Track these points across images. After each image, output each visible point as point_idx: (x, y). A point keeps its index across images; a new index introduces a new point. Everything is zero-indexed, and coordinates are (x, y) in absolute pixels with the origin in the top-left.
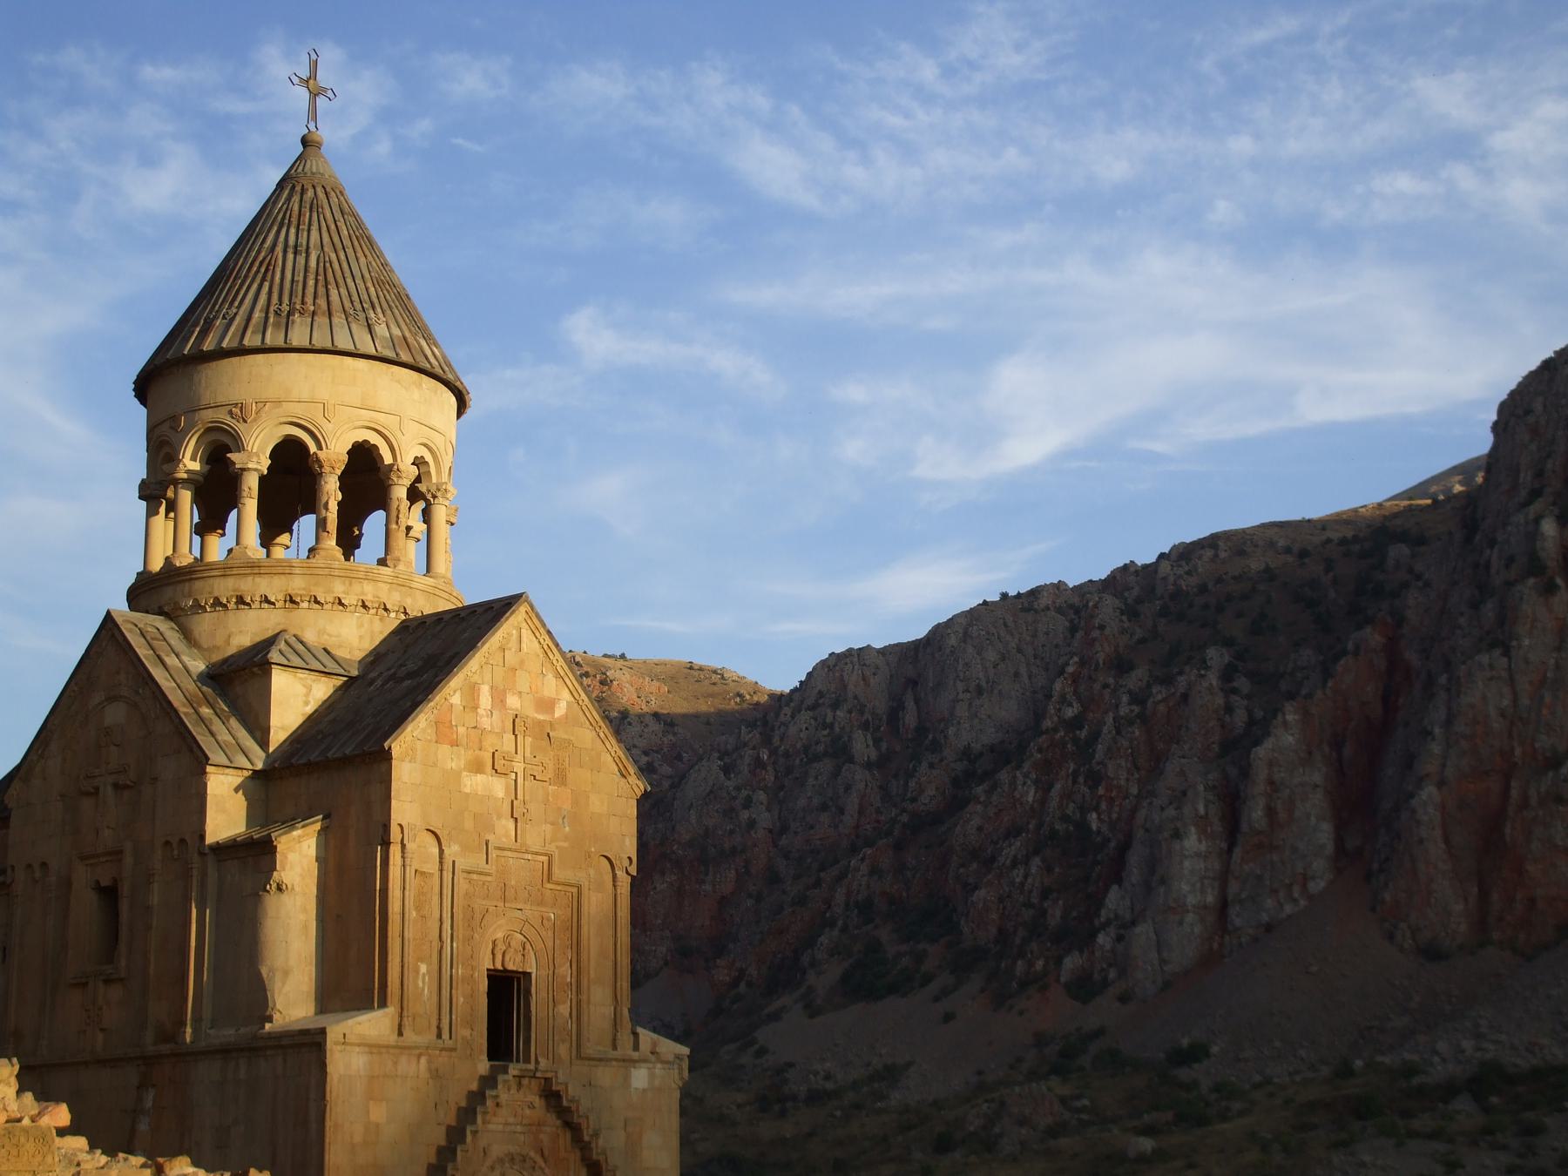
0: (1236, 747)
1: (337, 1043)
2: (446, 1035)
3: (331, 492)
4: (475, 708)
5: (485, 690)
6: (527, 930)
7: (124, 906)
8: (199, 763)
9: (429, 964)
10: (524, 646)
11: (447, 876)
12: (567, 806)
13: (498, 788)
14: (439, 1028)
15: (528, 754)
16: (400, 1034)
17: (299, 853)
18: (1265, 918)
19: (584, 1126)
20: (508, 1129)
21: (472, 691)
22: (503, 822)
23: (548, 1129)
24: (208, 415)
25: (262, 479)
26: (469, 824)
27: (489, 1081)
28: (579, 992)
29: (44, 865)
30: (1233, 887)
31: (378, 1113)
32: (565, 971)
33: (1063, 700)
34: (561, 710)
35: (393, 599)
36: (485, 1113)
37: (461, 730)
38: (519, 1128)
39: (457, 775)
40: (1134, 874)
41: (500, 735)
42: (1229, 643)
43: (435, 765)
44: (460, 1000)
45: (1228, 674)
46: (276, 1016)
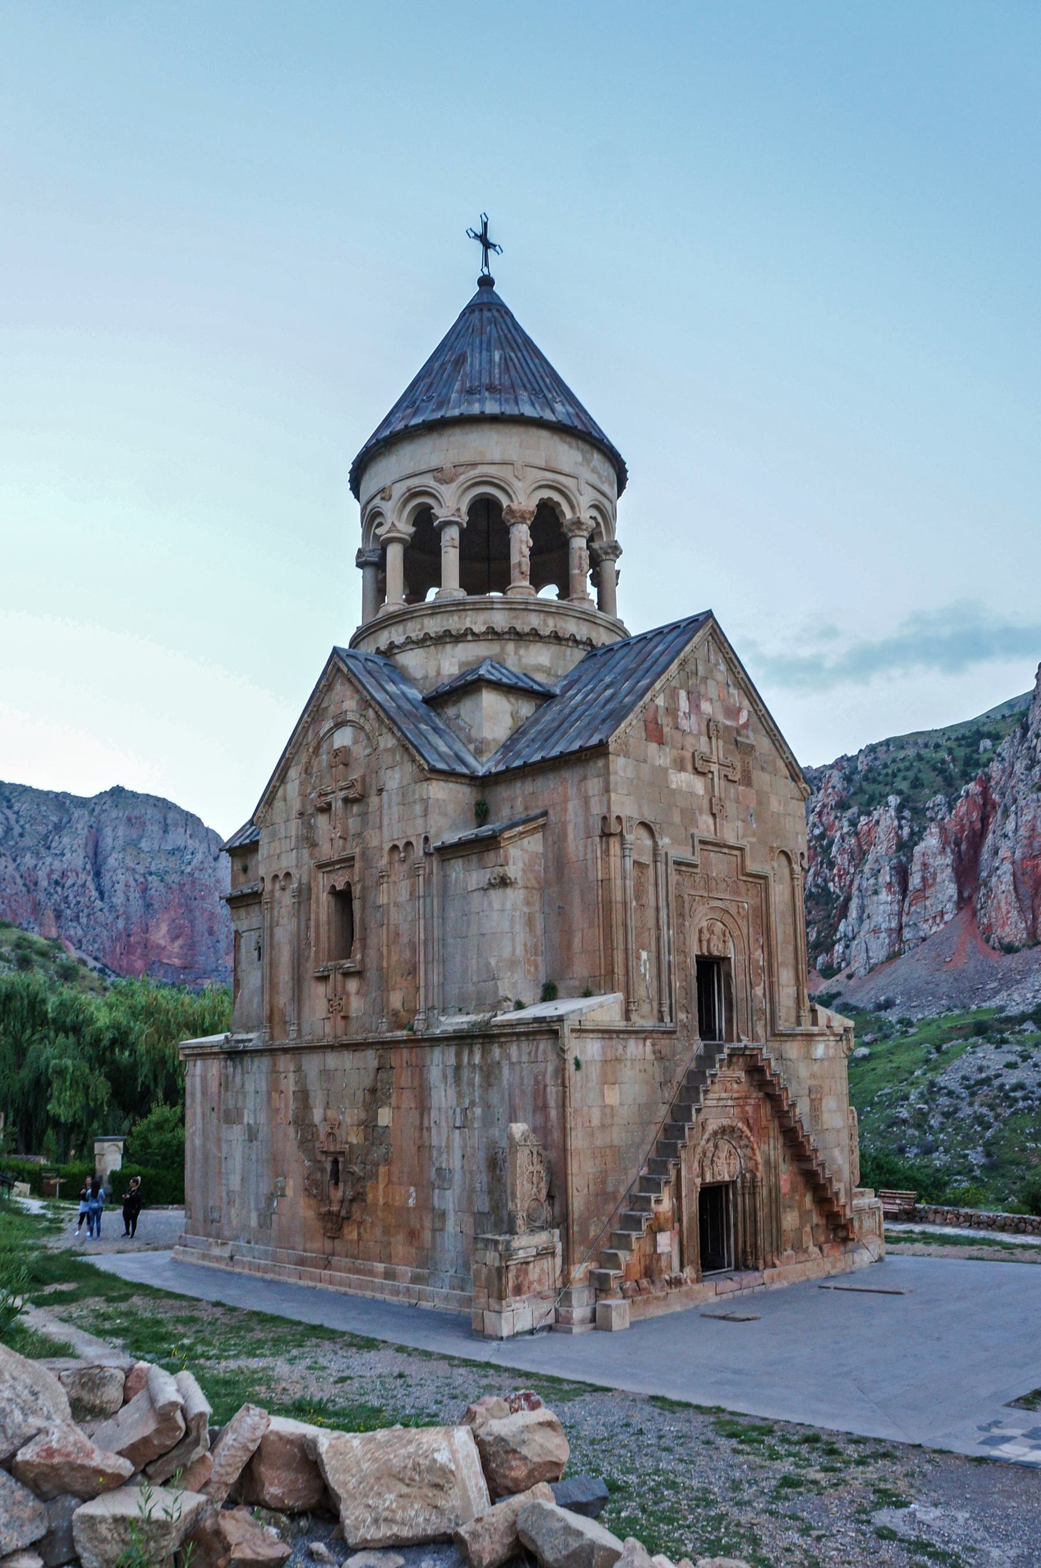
0: (905, 847)
1: (573, 1031)
2: (667, 1019)
7: (356, 905)
9: (649, 952)
11: (661, 867)
12: (753, 805)
14: (660, 1012)
15: (721, 756)
16: (628, 1019)
18: (922, 934)
20: (721, 1103)
23: (752, 1101)
25: (463, 533)
27: (706, 1060)
30: (904, 919)
32: (759, 955)
33: (814, 825)
34: (743, 719)
38: (730, 1103)
39: (665, 770)
40: (853, 913)
42: (899, 793)
43: (645, 761)
44: (677, 984)
45: (900, 809)
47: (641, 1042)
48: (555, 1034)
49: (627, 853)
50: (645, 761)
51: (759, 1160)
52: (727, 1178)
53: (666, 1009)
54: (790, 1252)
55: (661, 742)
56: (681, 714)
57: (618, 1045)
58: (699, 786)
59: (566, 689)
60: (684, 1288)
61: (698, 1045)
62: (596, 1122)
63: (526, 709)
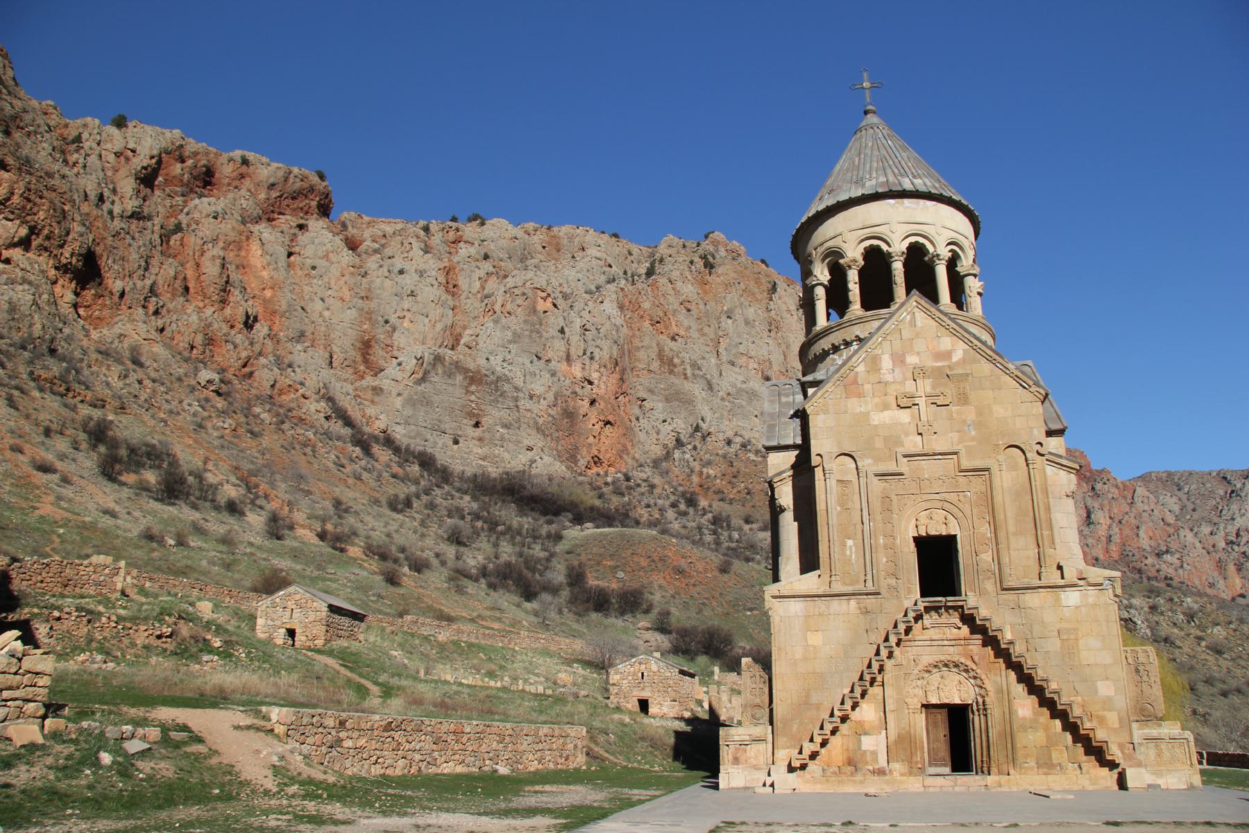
6: (947, 506)
10: (919, 324)
22: (911, 437)
26: (879, 444)
31: (815, 639)
37: (867, 387)
39: (866, 415)
41: (902, 383)
43: (846, 412)
47: (844, 603)
50: (846, 412)
52: (957, 701)
53: (869, 577)
57: (821, 604)
58: (905, 416)
62: (798, 656)
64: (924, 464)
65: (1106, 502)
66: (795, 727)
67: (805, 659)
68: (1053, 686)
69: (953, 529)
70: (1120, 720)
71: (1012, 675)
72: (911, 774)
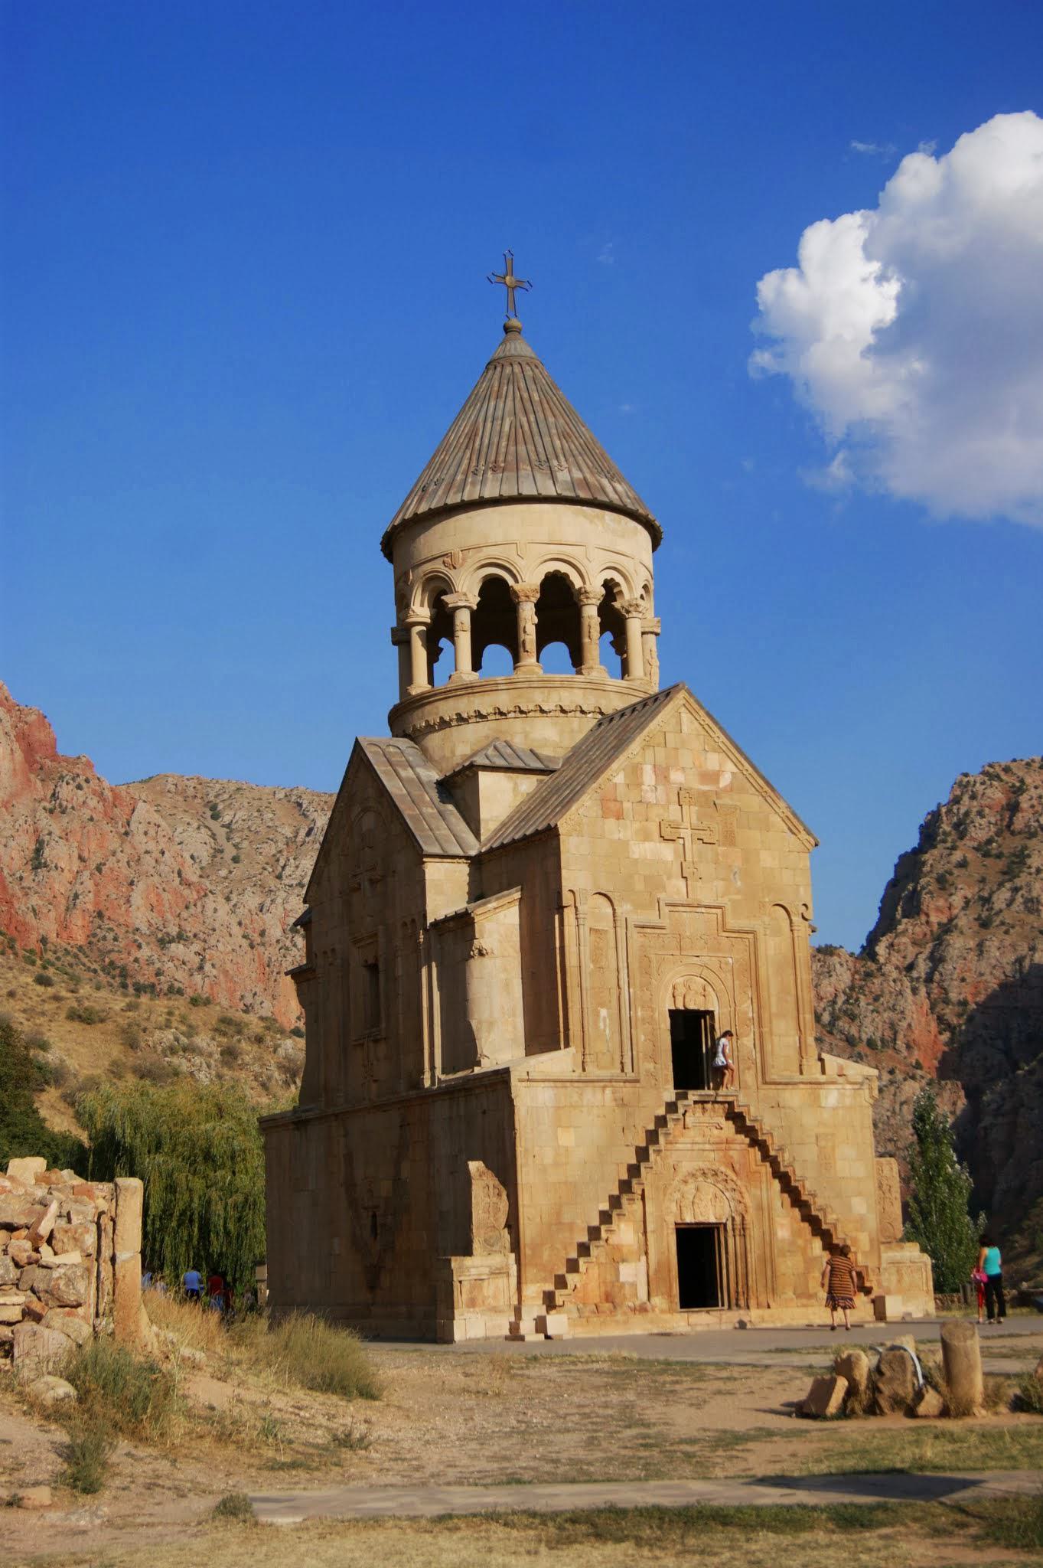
1: (521, 1080)
2: (628, 1068)
3: (528, 617)
4: (640, 784)
5: (648, 769)
6: (706, 973)
7: (382, 976)
8: (419, 857)
10: (685, 728)
11: (621, 932)
13: (667, 852)
17: (500, 924)
19: (769, 1142)
20: (696, 1147)
21: (635, 771)
24: (428, 567)
25: (475, 616)
26: (639, 886)
27: (672, 1107)
28: (760, 1025)
29: (333, 950)
31: (567, 1138)
32: (747, 1008)
35: (589, 702)
36: (667, 1134)
37: (627, 805)
39: (624, 844)
44: (641, 1037)
46: (484, 1061)
48: (506, 1083)
49: (581, 921)
51: (749, 1204)
52: (713, 1220)
53: (627, 1060)
54: (790, 1294)
55: (619, 816)
56: (644, 787)
59: (567, 761)
60: (650, 1315)
61: (670, 1094)
63: (528, 784)
64: (686, 916)
65: (76, 825)
66: (546, 1255)
67: (556, 1164)
68: (820, 1201)
69: (712, 1005)
70: (871, 1241)
71: (776, 1185)
72: (671, 1311)
